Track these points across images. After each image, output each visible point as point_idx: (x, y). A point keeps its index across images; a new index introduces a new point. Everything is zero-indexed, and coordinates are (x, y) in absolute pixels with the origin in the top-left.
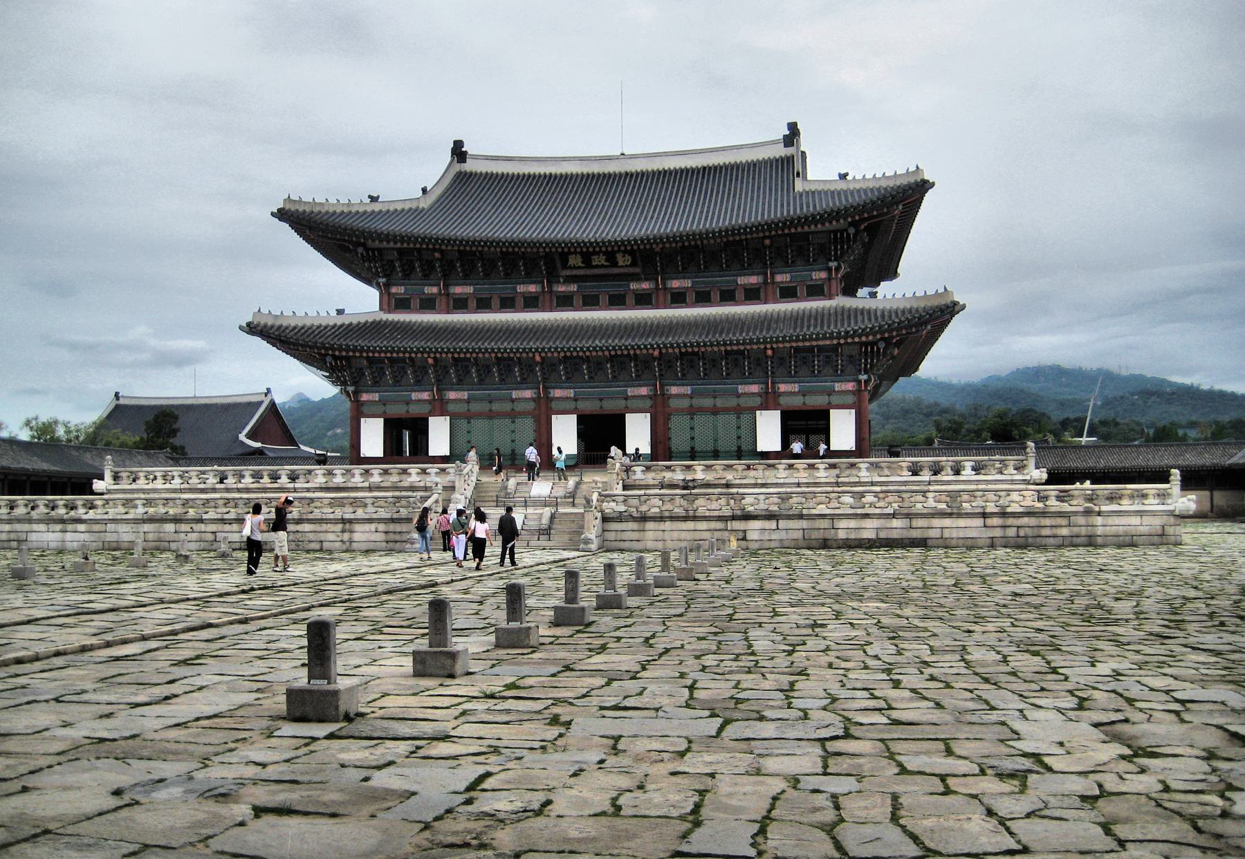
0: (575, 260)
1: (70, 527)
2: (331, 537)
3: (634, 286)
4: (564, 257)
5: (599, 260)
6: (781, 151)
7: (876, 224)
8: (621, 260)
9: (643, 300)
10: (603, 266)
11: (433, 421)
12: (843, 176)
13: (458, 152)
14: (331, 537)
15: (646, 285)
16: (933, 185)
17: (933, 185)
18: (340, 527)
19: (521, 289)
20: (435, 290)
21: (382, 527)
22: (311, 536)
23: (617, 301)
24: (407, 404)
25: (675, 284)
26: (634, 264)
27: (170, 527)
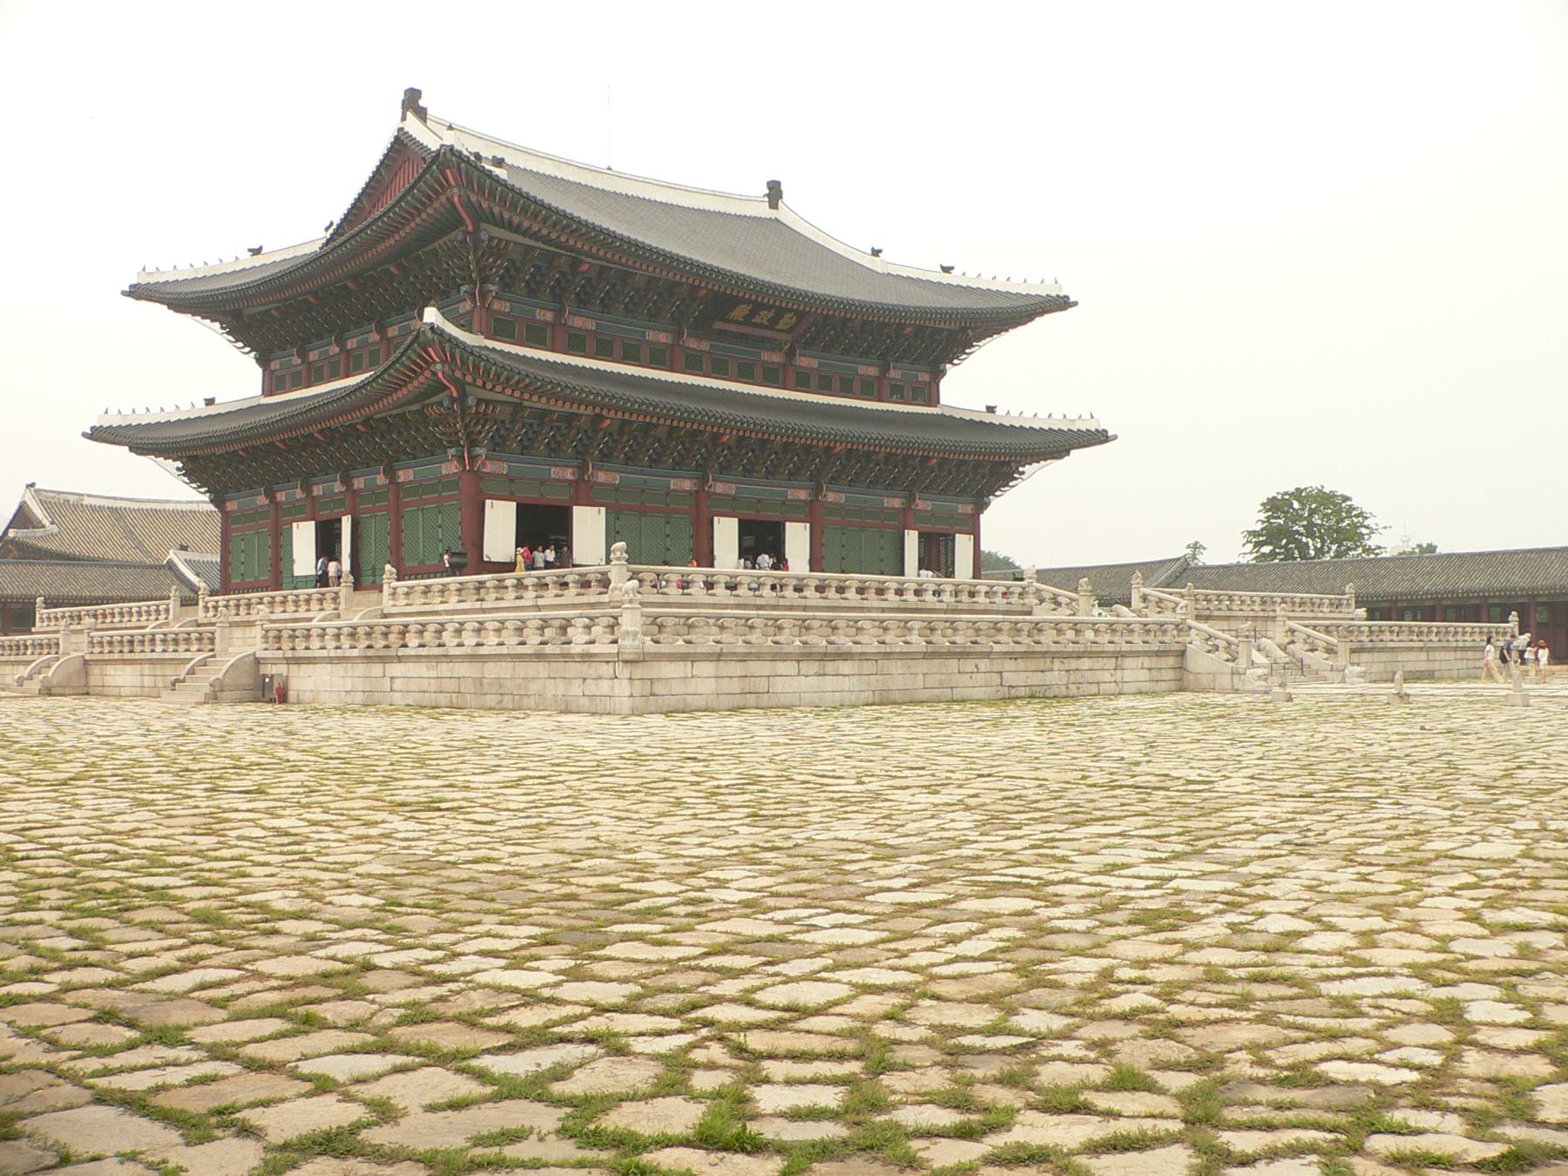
0: (741, 311)
1: (830, 667)
2: (1106, 676)
3: (765, 356)
4: (736, 301)
5: (763, 317)
6: (764, 211)
7: (945, 328)
8: (787, 321)
9: (771, 379)
10: (760, 326)
11: (578, 511)
12: (947, 270)
13: (412, 102)
14: (1106, 676)
15: (777, 358)
16: (1075, 304)
17: (1075, 304)
18: (1111, 663)
19: (651, 336)
20: (549, 316)
21: (1147, 661)
22: (1089, 676)
23: (745, 375)
24: (542, 483)
25: (805, 362)
26: (789, 331)
27: (953, 664)
